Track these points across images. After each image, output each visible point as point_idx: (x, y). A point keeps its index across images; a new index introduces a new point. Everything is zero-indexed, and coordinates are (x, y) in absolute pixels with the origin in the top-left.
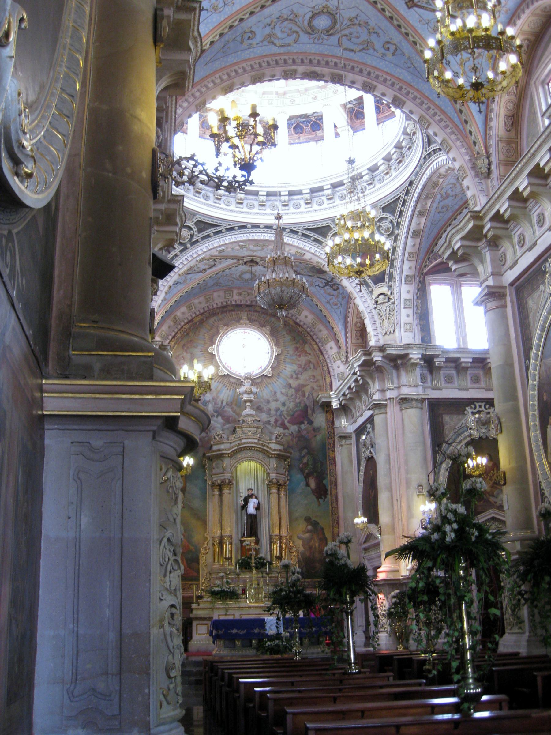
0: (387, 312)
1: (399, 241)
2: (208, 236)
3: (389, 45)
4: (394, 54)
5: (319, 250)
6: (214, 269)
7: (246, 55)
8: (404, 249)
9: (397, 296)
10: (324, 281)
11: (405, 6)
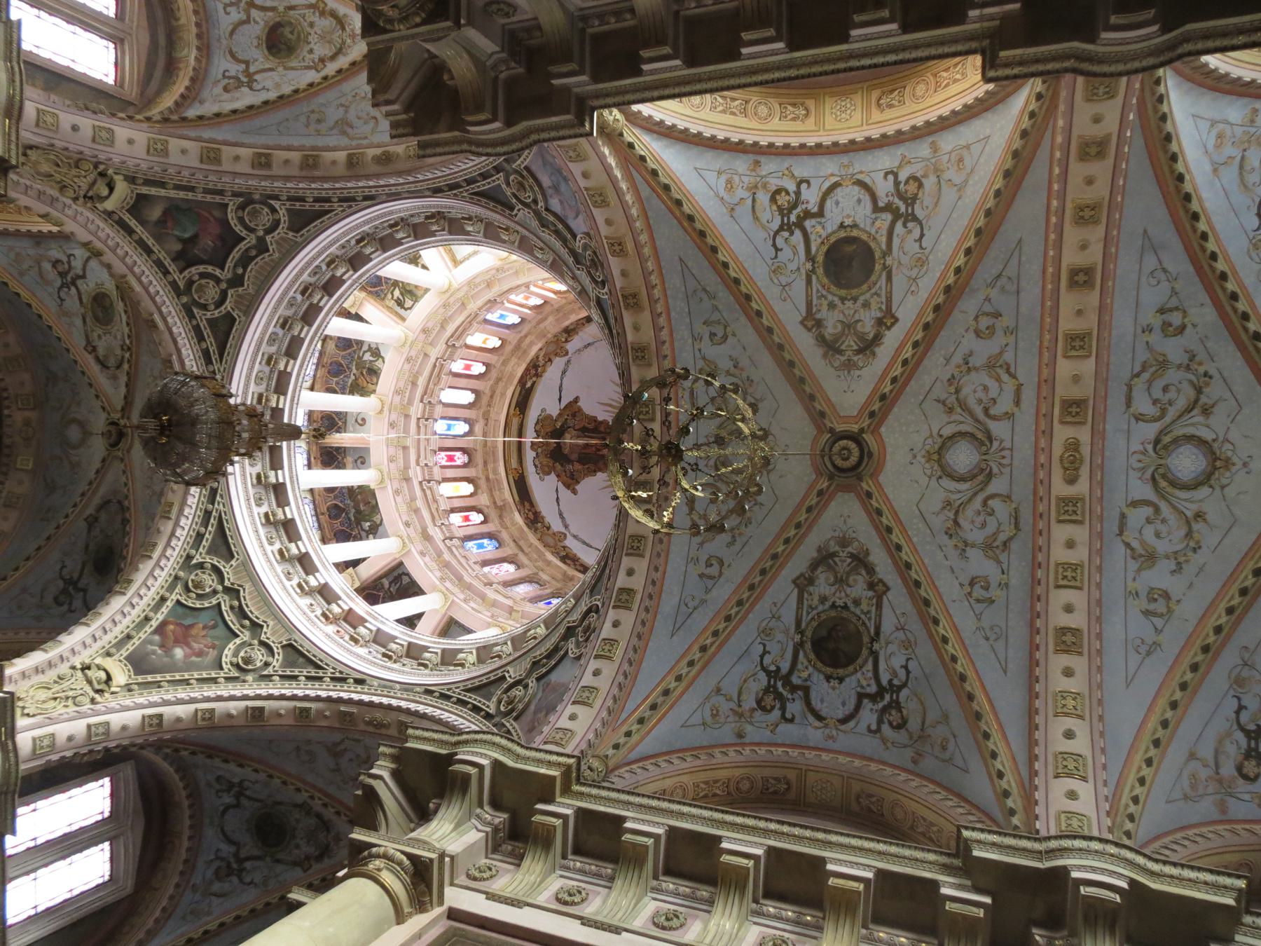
0: (71, 693)
1: (230, 685)
2: (201, 338)
3: (716, 567)
4: (701, 576)
5: (180, 544)
6: (96, 368)
7: (682, 333)
8: (219, 699)
9: (113, 705)
10: (76, 576)
11: (797, 573)
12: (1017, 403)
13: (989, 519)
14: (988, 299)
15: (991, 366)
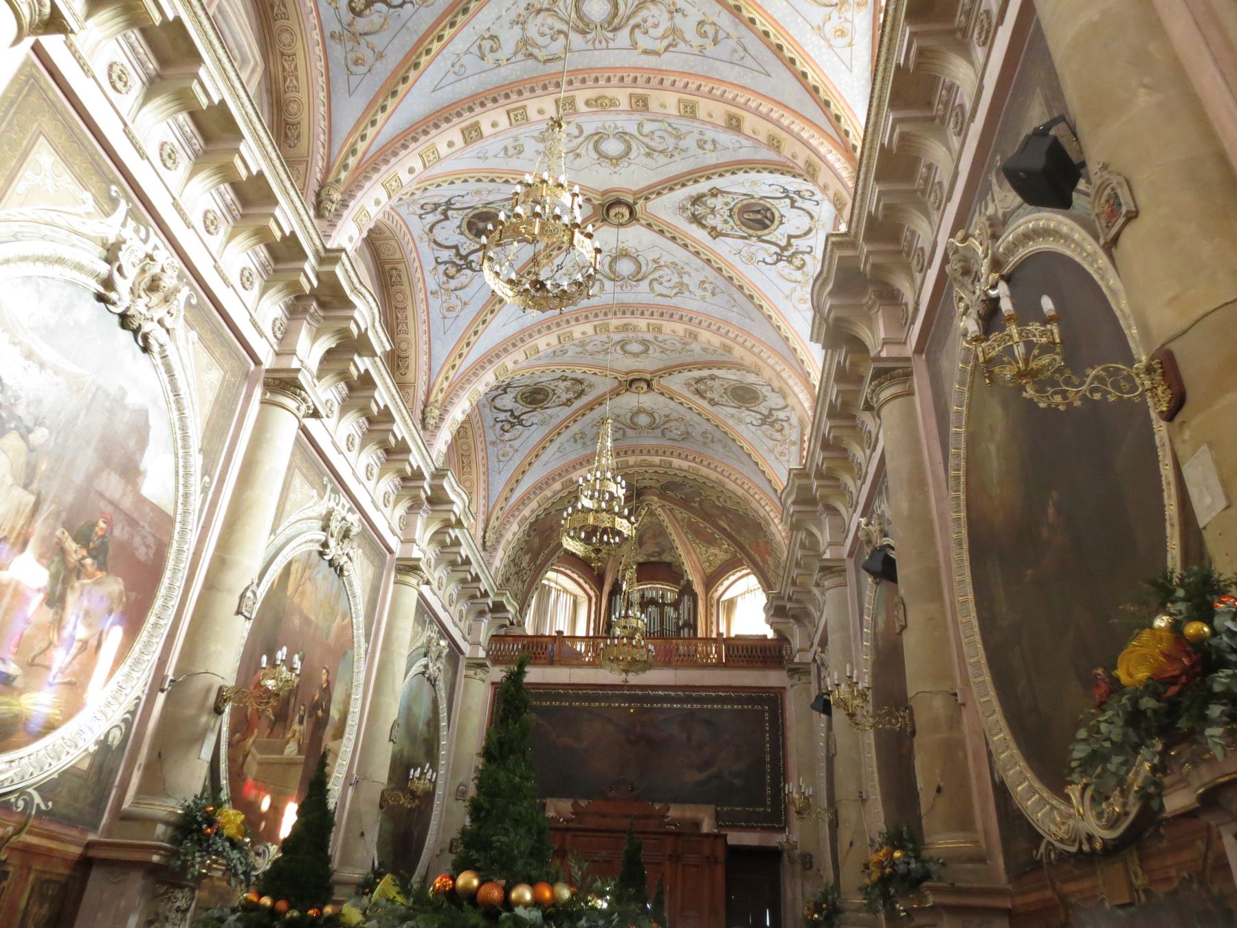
12: (645, 52)
13: (548, 38)
14: (728, 36)
15: (674, 30)
